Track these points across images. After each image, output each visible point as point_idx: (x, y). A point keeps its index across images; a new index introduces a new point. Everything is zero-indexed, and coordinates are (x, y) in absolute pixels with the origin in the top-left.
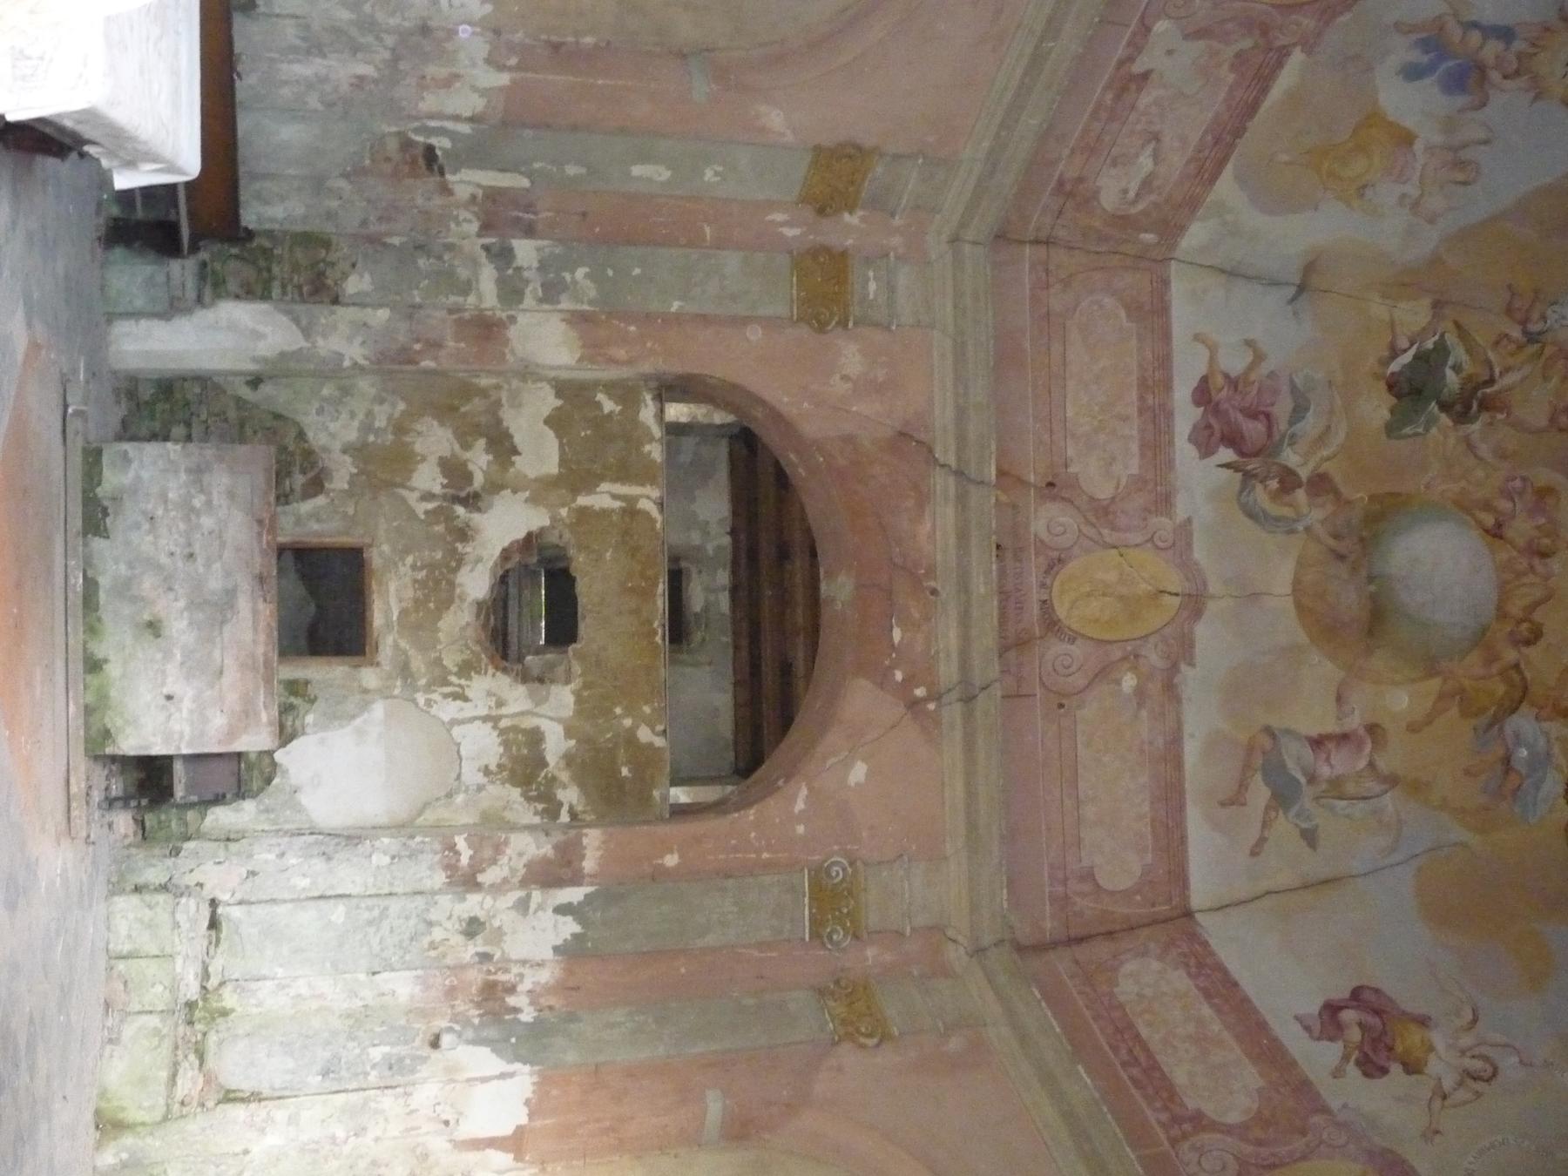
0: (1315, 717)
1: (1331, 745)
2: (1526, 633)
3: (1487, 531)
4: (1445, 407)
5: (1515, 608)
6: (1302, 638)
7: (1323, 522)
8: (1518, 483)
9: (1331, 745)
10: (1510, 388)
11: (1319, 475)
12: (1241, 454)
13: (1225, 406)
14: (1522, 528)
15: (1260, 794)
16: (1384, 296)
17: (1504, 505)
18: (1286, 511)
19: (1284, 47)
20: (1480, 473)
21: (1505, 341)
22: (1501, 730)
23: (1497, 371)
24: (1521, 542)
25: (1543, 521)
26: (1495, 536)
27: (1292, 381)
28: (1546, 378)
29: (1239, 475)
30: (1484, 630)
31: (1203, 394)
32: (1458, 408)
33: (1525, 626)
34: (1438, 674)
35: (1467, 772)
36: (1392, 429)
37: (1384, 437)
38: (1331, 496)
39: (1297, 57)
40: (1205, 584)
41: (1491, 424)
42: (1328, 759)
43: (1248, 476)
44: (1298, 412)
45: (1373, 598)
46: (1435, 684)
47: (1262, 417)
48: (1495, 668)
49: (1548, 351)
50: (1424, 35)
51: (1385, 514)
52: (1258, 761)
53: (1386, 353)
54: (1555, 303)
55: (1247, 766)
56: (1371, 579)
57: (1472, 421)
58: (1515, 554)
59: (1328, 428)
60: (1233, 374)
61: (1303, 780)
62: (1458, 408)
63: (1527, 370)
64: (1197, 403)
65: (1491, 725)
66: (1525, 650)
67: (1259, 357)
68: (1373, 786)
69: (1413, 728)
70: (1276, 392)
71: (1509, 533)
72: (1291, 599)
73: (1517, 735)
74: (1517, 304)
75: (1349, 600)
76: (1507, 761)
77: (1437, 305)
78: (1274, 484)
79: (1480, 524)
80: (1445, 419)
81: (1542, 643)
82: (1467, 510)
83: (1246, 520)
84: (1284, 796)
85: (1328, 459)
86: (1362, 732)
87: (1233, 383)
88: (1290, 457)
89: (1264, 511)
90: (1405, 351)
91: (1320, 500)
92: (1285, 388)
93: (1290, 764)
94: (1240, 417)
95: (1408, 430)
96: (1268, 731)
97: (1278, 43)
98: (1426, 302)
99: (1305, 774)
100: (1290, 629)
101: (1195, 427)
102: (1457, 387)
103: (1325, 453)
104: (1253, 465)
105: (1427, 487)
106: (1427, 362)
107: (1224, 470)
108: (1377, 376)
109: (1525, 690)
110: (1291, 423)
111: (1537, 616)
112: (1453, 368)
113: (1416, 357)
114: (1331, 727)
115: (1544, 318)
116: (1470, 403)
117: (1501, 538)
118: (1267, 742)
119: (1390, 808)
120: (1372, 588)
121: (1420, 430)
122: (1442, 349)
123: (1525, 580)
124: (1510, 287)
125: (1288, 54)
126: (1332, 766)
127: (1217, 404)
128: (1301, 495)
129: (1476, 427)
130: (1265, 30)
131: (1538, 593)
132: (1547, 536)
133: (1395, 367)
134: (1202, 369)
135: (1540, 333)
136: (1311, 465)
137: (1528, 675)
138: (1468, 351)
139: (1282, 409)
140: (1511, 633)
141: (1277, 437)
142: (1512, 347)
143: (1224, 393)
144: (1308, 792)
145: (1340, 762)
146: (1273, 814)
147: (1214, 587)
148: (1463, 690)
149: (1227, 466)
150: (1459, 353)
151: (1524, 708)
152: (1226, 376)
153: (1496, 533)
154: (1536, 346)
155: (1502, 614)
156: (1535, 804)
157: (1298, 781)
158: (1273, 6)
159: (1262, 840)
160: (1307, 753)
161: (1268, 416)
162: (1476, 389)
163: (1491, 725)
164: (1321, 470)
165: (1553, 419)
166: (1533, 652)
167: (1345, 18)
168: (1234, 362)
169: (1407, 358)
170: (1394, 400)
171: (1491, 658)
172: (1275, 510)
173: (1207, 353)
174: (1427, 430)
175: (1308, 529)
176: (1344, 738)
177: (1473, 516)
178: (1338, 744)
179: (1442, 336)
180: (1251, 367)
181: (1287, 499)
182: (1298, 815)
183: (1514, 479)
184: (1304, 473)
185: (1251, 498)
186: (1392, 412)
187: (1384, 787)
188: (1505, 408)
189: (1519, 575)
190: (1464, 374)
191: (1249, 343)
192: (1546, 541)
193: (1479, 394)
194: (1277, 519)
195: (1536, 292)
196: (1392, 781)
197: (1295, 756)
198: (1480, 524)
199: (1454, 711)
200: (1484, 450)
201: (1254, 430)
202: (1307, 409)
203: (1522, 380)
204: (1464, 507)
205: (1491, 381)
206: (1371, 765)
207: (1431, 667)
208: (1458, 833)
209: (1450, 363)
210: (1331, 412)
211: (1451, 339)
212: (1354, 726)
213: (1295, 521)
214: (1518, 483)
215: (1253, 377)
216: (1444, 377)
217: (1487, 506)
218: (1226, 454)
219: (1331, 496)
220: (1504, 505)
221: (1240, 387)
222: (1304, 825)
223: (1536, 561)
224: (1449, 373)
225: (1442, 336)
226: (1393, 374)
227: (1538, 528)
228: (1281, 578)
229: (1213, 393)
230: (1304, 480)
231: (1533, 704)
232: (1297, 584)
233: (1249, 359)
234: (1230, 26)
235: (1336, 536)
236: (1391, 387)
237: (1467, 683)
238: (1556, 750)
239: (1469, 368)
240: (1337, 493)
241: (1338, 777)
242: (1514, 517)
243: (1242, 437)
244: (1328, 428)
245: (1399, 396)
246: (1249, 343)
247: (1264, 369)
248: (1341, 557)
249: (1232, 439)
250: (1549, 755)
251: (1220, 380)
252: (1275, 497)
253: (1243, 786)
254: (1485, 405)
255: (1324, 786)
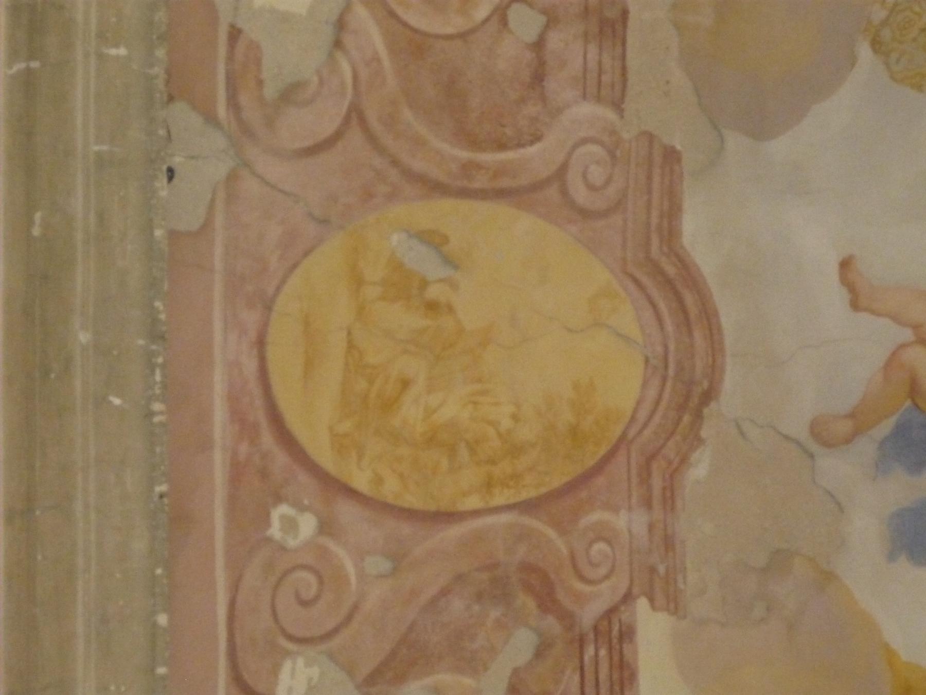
19: (611, 612)
39: (652, 628)
50: (886, 427)
97: (589, 615)
125: (628, 634)
130: (544, 590)
158: (528, 507)
167: (700, 469)
234: (457, 606)
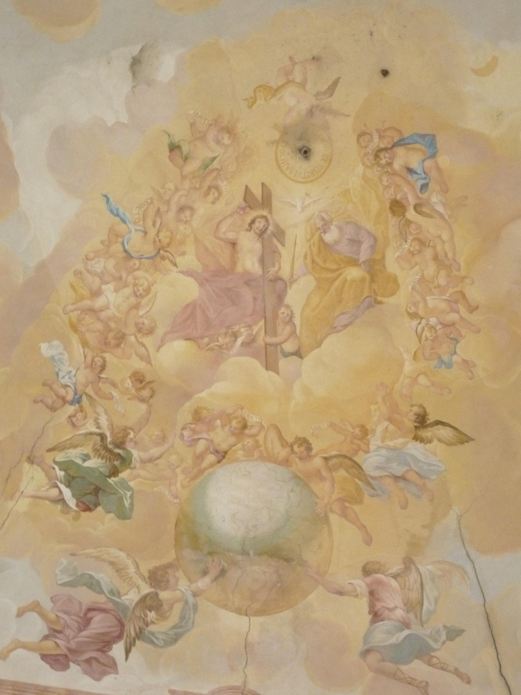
0: (355, 614)
1: (379, 605)
2: (302, 449)
3: (219, 462)
4: (115, 472)
5: (283, 453)
6: (287, 614)
7: (191, 581)
8: (186, 433)
9: (379, 605)
10: (111, 425)
11: (150, 578)
12: (119, 637)
13: (73, 645)
14: (221, 437)
15: (417, 668)
16: (12, 497)
17: (201, 446)
18: (177, 608)
20: (173, 458)
21: (74, 419)
22: (374, 478)
23: (94, 430)
24: (232, 440)
25: (218, 422)
26: (224, 457)
27: (64, 585)
28: (110, 398)
29: (138, 643)
30: (295, 477)
31: (58, 661)
32: (117, 463)
33: (296, 448)
34: (326, 517)
35: (404, 507)
36: (123, 514)
37: (127, 521)
38: (169, 571)
40: (231, 688)
41: (136, 443)
42: (389, 610)
43: (140, 635)
44: (93, 585)
45: (260, 554)
46: (334, 518)
47: (90, 615)
48: (324, 473)
49: (90, 390)
51: (193, 536)
52: (389, 666)
53: (59, 507)
54: (57, 374)
55: (394, 676)
56: (244, 553)
57: (130, 454)
58: (239, 445)
59: (112, 563)
60: (46, 632)
61: (406, 632)
62: (117, 463)
63: (100, 410)
64: (65, 667)
65: (369, 484)
66: (314, 452)
67: (35, 607)
68: (413, 576)
69: (368, 541)
70: (70, 599)
71: (224, 446)
72: (252, 618)
73: (378, 468)
74: (49, 401)
75: (260, 571)
76: (396, 478)
77: (31, 460)
78: (152, 615)
79: (212, 465)
80: (124, 475)
81: (312, 440)
82: (201, 472)
83: (180, 643)
84: (421, 651)
85: (137, 567)
86: (368, 580)
87: (54, 632)
88: (131, 598)
89: (175, 627)
90: (61, 492)
91: (172, 581)
92: (68, 590)
93: (393, 640)
94: (85, 633)
95: (127, 503)
96: (366, 653)
98: (26, 466)
99: (402, 630)
100: (276, 626)
101: (85, 672)
102: (100, 461)
103: (132, 570)
104: (131, 630)
105: (177, 497)
106: (73, 478)
107: (130, 655)
108: (76, 518)
109: (345, 457)
110: (101, 592)
111: (290, 439)
112: (84, 461)
113: (68, 486)
114: (364, 603)
115: (66, 386)
116: (116, 453)
117: (226, 453)
118: (372, 658)
119: (430, 567)
120: (252, 553)
121: (129, 494)
122: (65, 466)
123: (261, 442)
124: (36, 402)
126: (396, 607)
127: (69, 650)
128: (164, 595)
129: (136, 454)
131: (272, 435)
132: (230, 421)
133: (72, 503)
134: (35, 658)
135: (76, 394)
136: (140, 582)
137: (334, 453)
138: (75, 446)
139: (86, 597)
140: (301, 459)
141: (110, 606)
142: (80, 415)
143: (60, 642)
144: (416, 629)
145: (393, 600)
146: (435, 660)
147: (236, 681)
148: (342, 500)
149: (128, 652)
150: (74, 455)
151: (356, 459)
152: (46, 638)
153: (222, 456)
154: (84, 397)
155: (286, 462)
156: (430, 465)
157: (408, 636)
159: (457, 672)
160: (383, 626)
161: (89, 610)
162: (106, 448)
163: (369, 484)
164: (146, 575)
165: (142, 400)
166: (317, 446)
168: (35, 628)
169: (67, 493)
170: (100, 509)
171: (318, 475)
172: (174, 618)
173: (20, 652)
174: (130, 489)
175: (195, 595)
176: (372, 593)
177: (206, 469)
178: (378, 600)
179: (55, 462)
180: (43, 615)
181: (165, 607)
182: (436, 641)
183: (182, 436)
184: (146, 589)
185: (161, 637)
186: (108, 512)
187: (414, 570)
188: (125, 431)
189: (257, 445)
190: (92, 454)
191: (20, 613)
192: (234, 423)
193: (110, 446)
194: (182, 618)
195: (44, 385)
196: (408, 563)
197: (385, 635)
198: (212, 465)
199: (357, 508)
200: (154, 452)
201: (99, 624)
202: (91, 577)
203: (106, 412)
204: (198, 473)
205: (102, 436)
206: (395, 577)
207: (321, 520)
208: (450, 521)
209: (79, 461)
210: (97, 558)
211: (60, 457)
212: (364, 585)
213: (186, 602)
214: (186, 433)
215: (52, 616)
216: (88, 468)
217: (200, 458)
218: (117, 650)
219: (169, 571)
220: (201, 446)
221: (58, 628)
222: (444, 637)
223: (247, 431)
224: (87, 464)
225: (55, 462)
226: (77, 505)
227: (223, 426)
228: (232, 622)
229: (59, 652)
230: (152, 590)
231: (356, 452)
232: (239, 611)
233: (33, 616)
235: (205, 573)
236: (88, 509)
237: (335, 496)
238: (391, 444)
239: (87, 450)
240: (169, 566)
241: (405, 605)
242: (212, 441)
243: (103, 634)
244: (112, 563)
245: (97, 505)
246: (20, 613)
247: (47, 605)
248: (223, 572)
249: (105, 643)
250: (393, 449)
251: (49, 644)
252: (163, 616)
253: (410, 682)
254: (120, 445)
255: (411, 615)
